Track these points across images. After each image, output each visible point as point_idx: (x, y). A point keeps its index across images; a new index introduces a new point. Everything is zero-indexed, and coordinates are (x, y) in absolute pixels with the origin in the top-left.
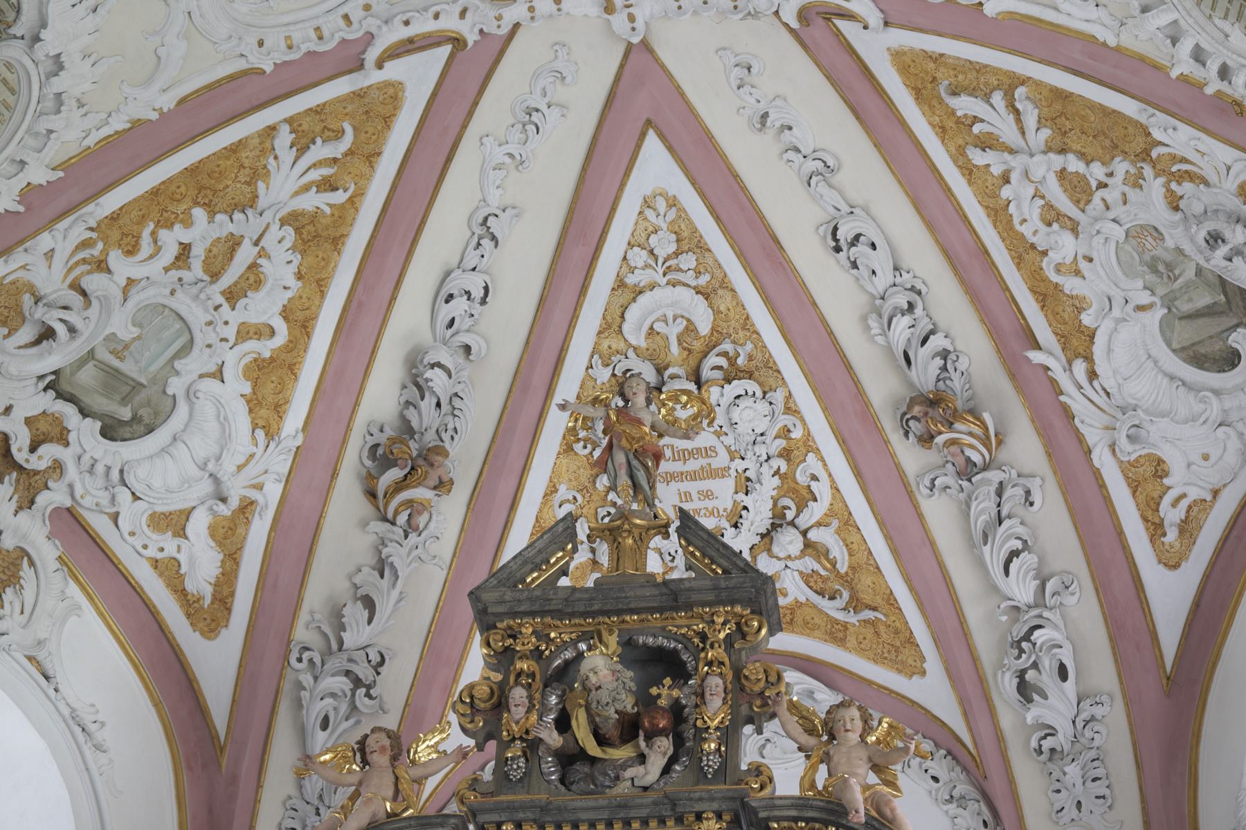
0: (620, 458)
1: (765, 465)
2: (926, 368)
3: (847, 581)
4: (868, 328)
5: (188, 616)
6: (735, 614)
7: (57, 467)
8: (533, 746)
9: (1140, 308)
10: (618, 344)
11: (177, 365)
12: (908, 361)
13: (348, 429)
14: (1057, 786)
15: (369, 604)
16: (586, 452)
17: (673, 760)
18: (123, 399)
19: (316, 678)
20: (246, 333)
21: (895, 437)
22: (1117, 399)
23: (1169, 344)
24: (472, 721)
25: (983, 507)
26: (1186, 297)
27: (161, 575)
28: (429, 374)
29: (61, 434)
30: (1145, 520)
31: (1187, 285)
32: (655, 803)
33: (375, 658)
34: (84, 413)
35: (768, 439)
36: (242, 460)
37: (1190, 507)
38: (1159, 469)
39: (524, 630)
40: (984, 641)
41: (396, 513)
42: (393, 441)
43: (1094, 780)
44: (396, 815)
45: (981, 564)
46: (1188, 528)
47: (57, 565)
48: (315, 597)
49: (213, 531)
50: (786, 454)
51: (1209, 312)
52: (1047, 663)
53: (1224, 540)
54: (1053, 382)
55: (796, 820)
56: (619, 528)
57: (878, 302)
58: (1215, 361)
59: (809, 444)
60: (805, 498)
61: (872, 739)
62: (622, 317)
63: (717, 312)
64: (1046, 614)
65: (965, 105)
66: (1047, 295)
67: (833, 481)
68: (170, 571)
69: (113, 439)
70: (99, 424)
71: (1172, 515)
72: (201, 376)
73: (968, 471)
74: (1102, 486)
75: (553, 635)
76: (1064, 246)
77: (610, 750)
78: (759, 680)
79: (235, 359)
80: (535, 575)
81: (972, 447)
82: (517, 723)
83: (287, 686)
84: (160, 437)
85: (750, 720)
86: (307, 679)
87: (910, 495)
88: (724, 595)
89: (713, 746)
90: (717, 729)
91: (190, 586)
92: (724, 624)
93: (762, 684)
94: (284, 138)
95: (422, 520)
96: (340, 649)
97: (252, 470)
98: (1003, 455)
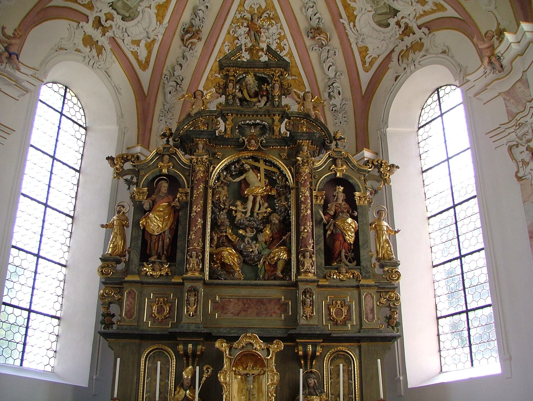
0: (252, 33)
1: (274, 41)
2: (315, 21)
4: (302, 11)
5: (139, 65)
6: (280, 71)
7: (111, 26)
8: (234, 97)
9: (368, 11)
10: (242, 9)
11: (140, 4)
12: (311, 19)
13: (178, 24)
14: (336, 118)
15: (181, 65)
16: (233, 34)
17: (267, 102)
18: (127, 11)
19: (168, 82)
21: (305, 37)
22: (359, 32)
23: (374, 20)
24: (219, 90)
25: (324, 55)
26: (380, 10)
27: (133, 55)
28: (198, 12)
29: (112, 18)
30: (362, 60)
31: (381, 7)
32: (264, 111)
33: (181, 78)
34: (118, 14)
35: (276, 35)
36: (153, 29)
37: (372, 59)
38: (367, 49)
39: (231, 70)
40: (321, 85)
41: (188, 45)
42: (189, 27)
43: (344, 117)
44: (203, 110)
45: (322, 68)
46: (371, 64)
47: (110, 50)
48: (168, 63)
49: (146, 45)
50: (279, 39)
51: (385, 14)
53: (379, 67)
54: (345, 27)
55: (297, 117)
56: (252, 49)
57: (305, 5)
58: (384, 25)
59: (285, 37)
60: (283, 49)
61: (313, 101)
62: (244, 2)
63: (267, 3)
64: (336, 80)
67: (289, 46)
68: (135, 54)
69: (124, 21)
70: (121, 17)
71: (368, 60)
72: (146, 7)
73: (322, 46)
74: (353, 52)
75: (237, 72)
77: (252, 99)
78: (286, 86)
80: (233, 58)
81: (323, 40)
82: (230, 91)
83: (161, 84)
84: (135, 21)
85: (284, 95)
86: (166, 82)
87: (307, 50)
88: (279, 65)
89: (277, 99)
90: (277, 96)
91: (140, 58)
92: (278, 72)
93: (287, 87)
95: (193, 47)
96: (173, 76)
97: (156, 31)
98: (330, 43)
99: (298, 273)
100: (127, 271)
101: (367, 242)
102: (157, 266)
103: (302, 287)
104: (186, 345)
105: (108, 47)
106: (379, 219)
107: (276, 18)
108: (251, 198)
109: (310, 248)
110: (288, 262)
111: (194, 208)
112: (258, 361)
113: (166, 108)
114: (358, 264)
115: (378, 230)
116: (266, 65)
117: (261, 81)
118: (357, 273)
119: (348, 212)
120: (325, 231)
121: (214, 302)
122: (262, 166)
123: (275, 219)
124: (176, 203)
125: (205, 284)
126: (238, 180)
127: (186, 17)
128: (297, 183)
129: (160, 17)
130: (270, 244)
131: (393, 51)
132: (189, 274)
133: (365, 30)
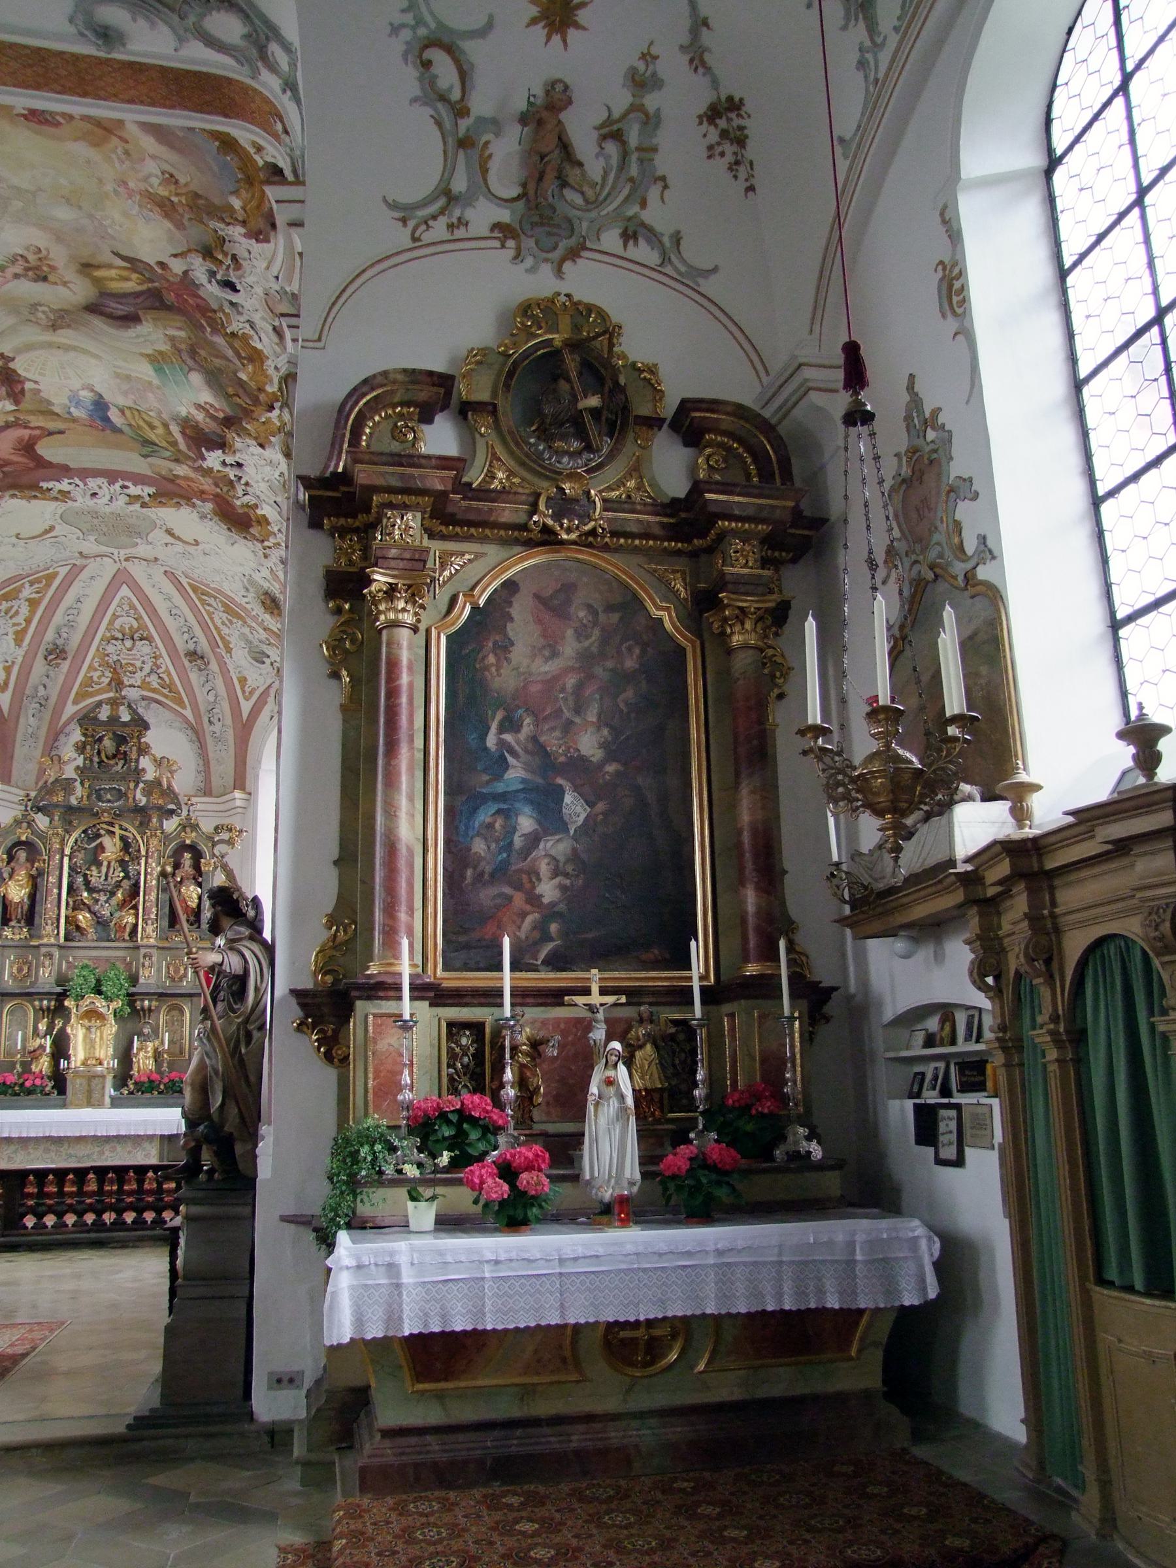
3: (169, 686)
20: (14, 625)
25: (203, 679)
38: (245, 679)
40: (202, 708)
46: (251, 693)
52: (216, 717)
60: (159, 667)
65: (204, 597)
66: (222, 638)
71: (247, 690)
79: (11, 631)
94: (27, 585)
98: (210, 667)
102: (17, 931)
103: (143, 951)
107: (148, 639)
108: (105, 863)
109: (153, 916)
110: (136, 926)
111: (51, 879)
112: (101, 1016)
113: (30, 730)
116: (125, 724)
117: (121, 740)
119: (194, 878)
121: (68, 962)
123: (126, 884)
124: (34, 872)
125: (60, 947)
126: (94, 844)
127: (50, 636)
128: (147, 852)
129: (19, 641)
130: (122, 906)
131: (270, 686)
132: (45, 941)
133: (243, 663)
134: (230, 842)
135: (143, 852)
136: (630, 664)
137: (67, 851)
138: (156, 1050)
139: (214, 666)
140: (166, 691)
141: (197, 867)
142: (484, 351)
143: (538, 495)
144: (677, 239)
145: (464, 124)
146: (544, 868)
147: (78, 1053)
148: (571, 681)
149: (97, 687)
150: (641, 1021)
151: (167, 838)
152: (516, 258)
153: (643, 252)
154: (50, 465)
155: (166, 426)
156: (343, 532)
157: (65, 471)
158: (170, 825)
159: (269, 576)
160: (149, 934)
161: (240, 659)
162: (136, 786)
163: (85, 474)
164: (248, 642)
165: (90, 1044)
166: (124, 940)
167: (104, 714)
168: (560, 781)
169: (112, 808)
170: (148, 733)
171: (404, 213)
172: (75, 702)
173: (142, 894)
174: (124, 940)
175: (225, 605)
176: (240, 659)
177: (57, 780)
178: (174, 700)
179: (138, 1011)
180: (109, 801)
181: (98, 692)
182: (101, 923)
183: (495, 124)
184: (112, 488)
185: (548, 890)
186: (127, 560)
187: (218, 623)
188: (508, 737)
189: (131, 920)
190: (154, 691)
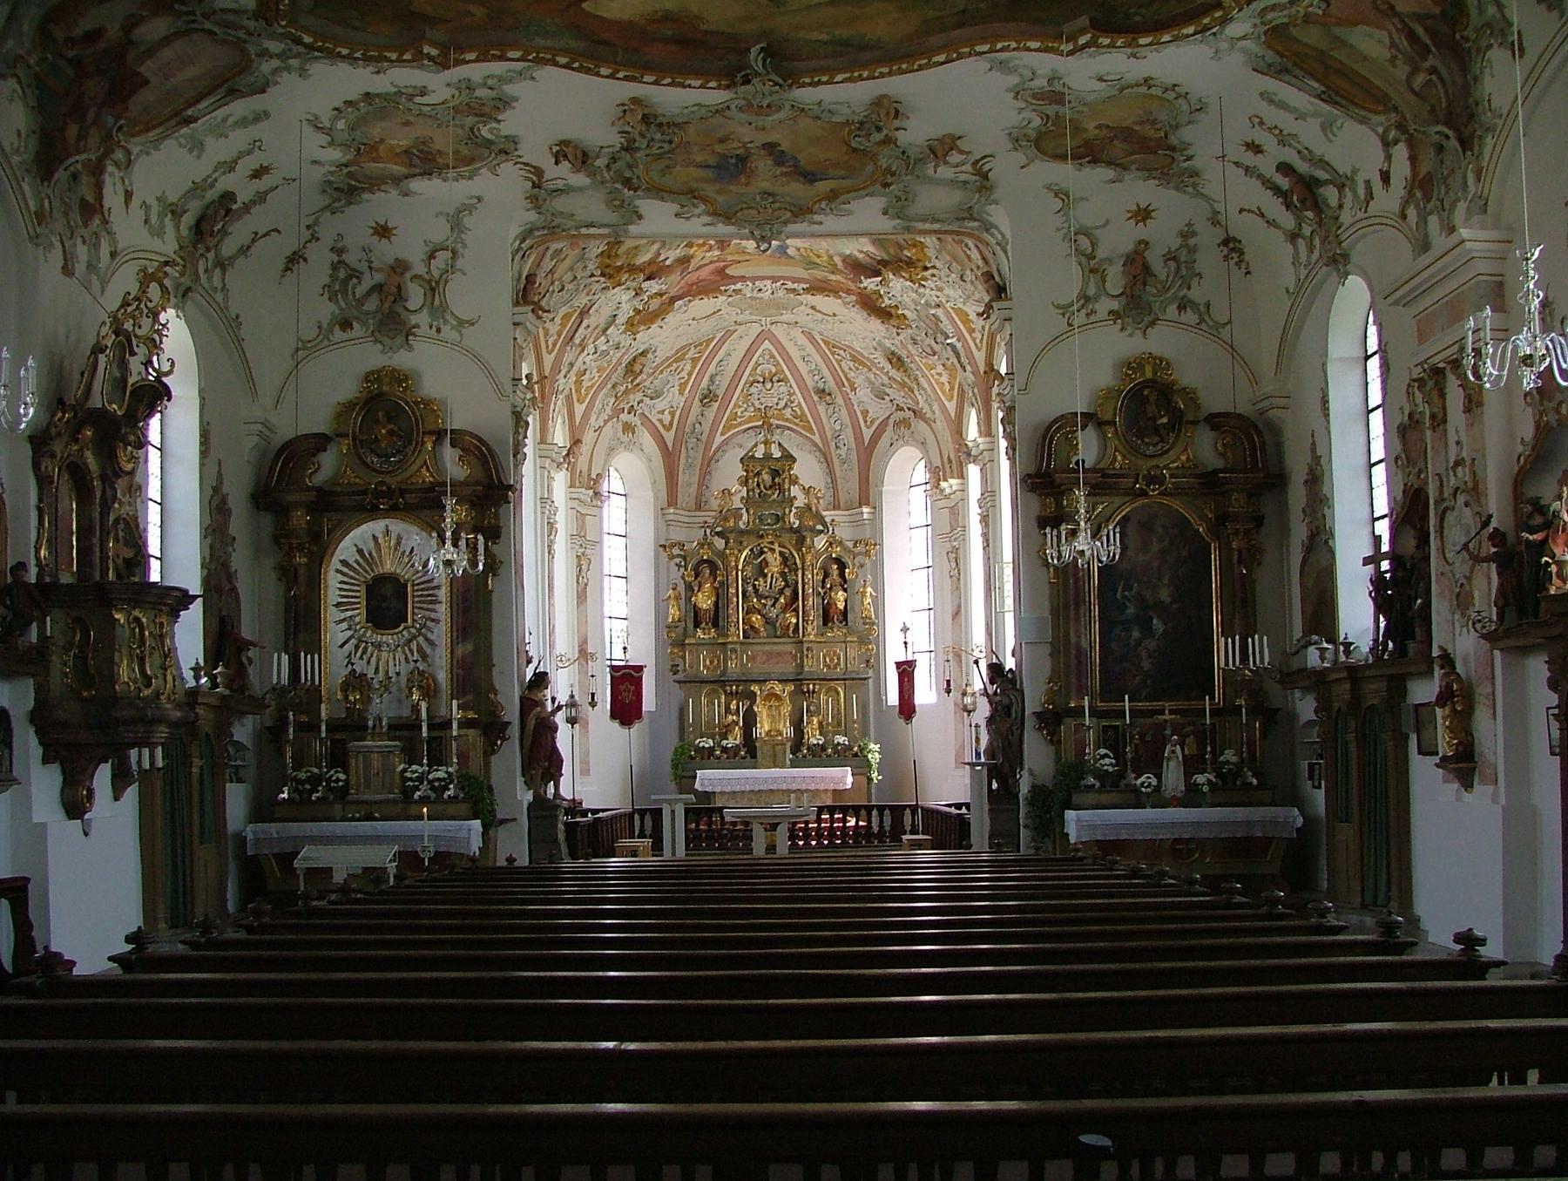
21: (813, 394)
38: (868, 412)
40: (829, 435)
52: (842, 442)
59: (794, 393)
66: (847, 379)
68: (660, 421)
71: (869, 420)
76: (853, 374)
99: (803, 636)
100: (685, 635)
101: (852, 608)
102: (706, 631)
103: (806, 645)
104: (731, 686)
105: (639, 423)
106: (865, 586)
108: (770, 575)
109: (811, 618)
110: (797, 624)
112: (778, 697)
113: (690, 460)
114: (847, 624)
115: (863, 594)
117: (775, 473)
118: (844, 631)
120: (823, 600)
122: (776, 546)
123: (788, 592)
124: (716, 585)
127: (705, 383)
129: (681, 393)
130: (785, 609)
131: (889, 417)
132: (730, 639)
133: (865, 399)
134: (867, 554)
135: (800, 566)
136: (1184, 553)
137: (740, 567)
138: (820, 723)
139: (840, 401)
140: (797, 421)
141: (842, 575)
142: (1109, 390)
143: (1138, 475)
144: (1208, 305)
145: (1092, 262)
146: (1144, 654)
147: (763, 727)
148: (1155, 564)
149: (739, 420)
150: (1189, 725)
151: (818, 554)
152: (1122, 329)
153: (1190, 317)
154: (732, 277)
155: (831, 257)
156: (1047, 495)
157: (743, 279)
158: (820, 542)
159: (899, 344)
160: (812, 631)
161: (863, 395)
162: (791, 511)
163: (754, 279)
164: (870, 382)
165: (773, 719)
166: (789, 637)
167: (759, 454)
168: (1151, 613)
169: (775, 530)
170: (795, 466)
171: (1064, 309)
172: (722, 434)
173: (800, 599)
174: (789, 637)
175: (851, 355)
176: (863, 395)
177: (728, 510)
178: (803, 427)
179: (804, 693)
180: (768, 524)
181: (740, 424)
182: (768, 621)
183: (1109, 260)
184: (774, 285)
185: (1146, 665)
186: (772, 324)
187: (846, 369)
188: (1126, 593)
189: (794, 621)
190: (787, 420)
